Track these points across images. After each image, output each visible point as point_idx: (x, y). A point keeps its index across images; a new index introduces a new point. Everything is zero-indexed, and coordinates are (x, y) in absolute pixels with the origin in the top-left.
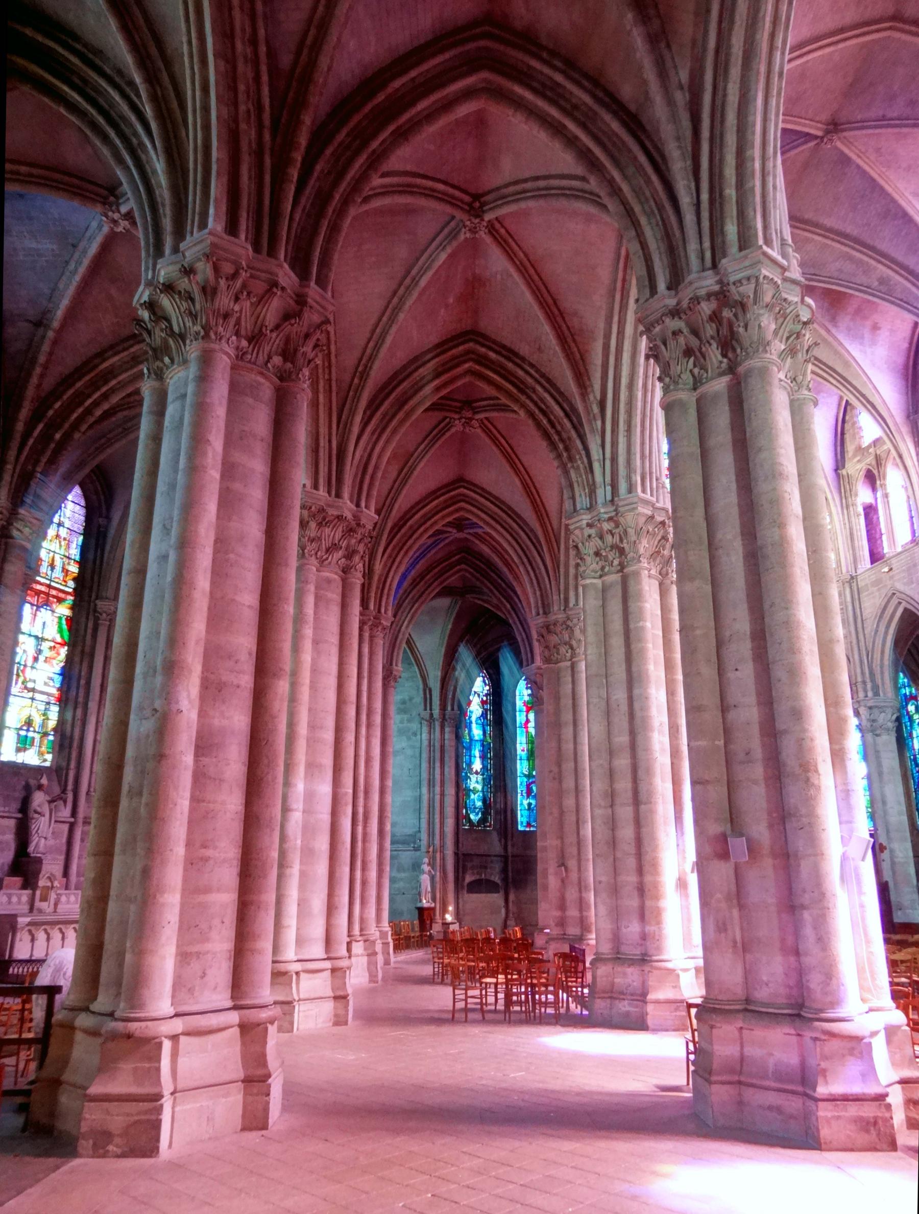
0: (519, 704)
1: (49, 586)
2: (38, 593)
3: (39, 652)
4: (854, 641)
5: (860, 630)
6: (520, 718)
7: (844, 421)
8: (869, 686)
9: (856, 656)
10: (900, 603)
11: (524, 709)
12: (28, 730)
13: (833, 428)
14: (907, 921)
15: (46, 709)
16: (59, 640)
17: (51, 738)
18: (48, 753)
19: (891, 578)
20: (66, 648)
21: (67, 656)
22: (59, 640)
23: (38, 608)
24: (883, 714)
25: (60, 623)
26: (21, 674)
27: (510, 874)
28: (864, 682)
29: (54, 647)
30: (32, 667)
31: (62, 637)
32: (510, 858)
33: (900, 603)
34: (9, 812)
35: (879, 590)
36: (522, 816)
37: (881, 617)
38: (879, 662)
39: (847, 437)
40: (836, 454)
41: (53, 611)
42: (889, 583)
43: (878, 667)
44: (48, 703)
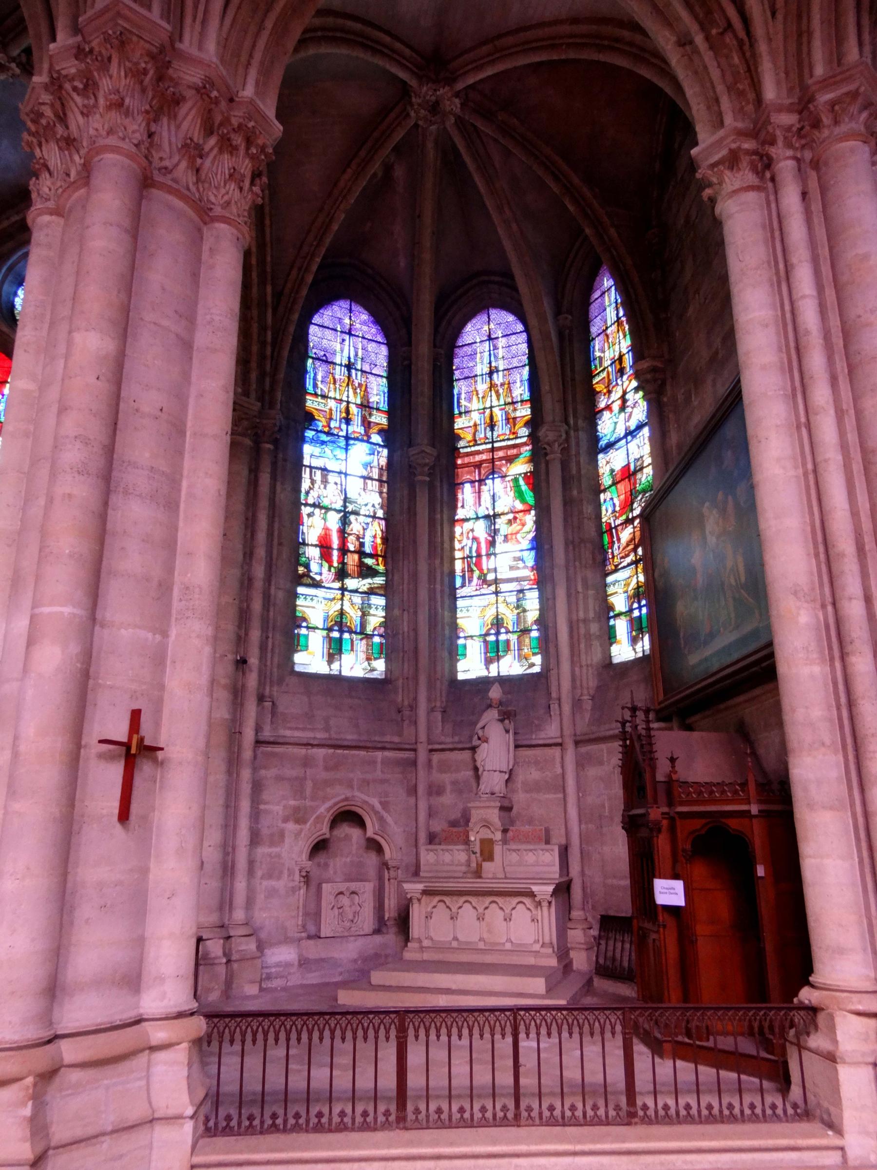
1: (493, 450)
2: (478, 465)
3: (496, 532)
12: (498, 633)
15: (518, 600)
16: (519, 506)
17: (535, 634)
18: (534, 654)
20: (533, 512)
21: (536, 522)
22: (519, 506)
23: (481, 482)
25: (517, 486)
26: (475, 568)
29: (515, 518)
30: (488, 555)
31: (523, 501)
34: (460, 742)
41: (503, 477)
44: (521, 591)
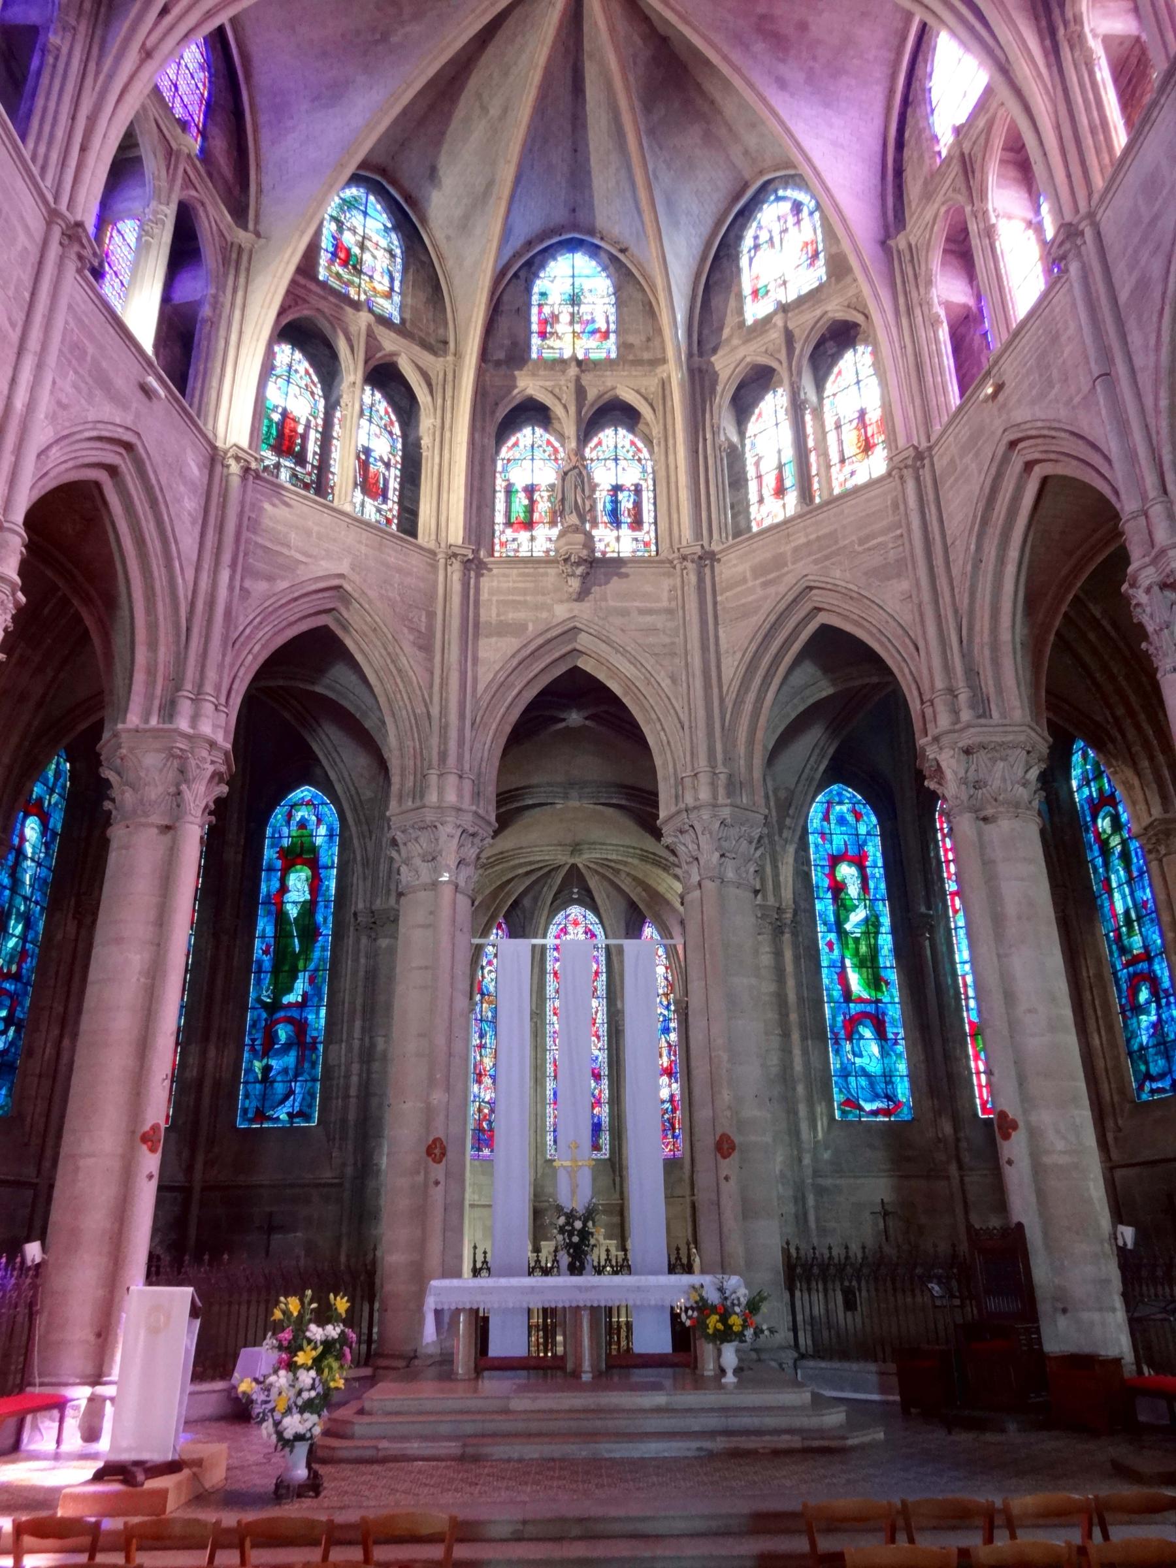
0: (269, 854)
4: (926, 596)
5: (940, 570)
6: (268, 886)
7: (900, 145)
8: (963, 697)
9: (932, 630)
10: (1029, 466)
11: (279, 864)
13: (877, 159)
14: (1087, 1350)
19: (1004, 406)
24: (1001, 764)
27: (192, 1232)
28: (951, 691)
32: (196, 1196)
33: (1029, 466)
35: (977, 455)
36: (247, 1096)
37: (985, 522)
38: (986, 639)
39: (908, 174)
40: (884, 214)
42: (998, 424)
43: (987, 652)
